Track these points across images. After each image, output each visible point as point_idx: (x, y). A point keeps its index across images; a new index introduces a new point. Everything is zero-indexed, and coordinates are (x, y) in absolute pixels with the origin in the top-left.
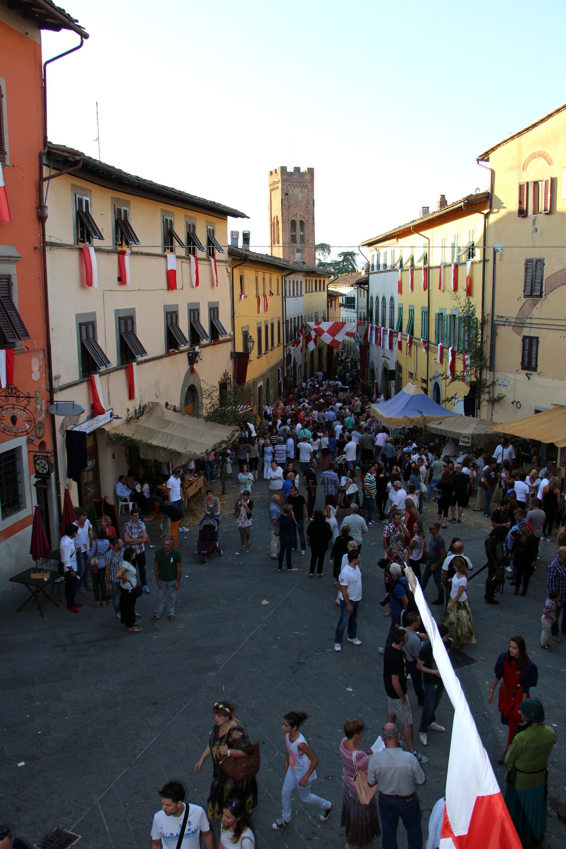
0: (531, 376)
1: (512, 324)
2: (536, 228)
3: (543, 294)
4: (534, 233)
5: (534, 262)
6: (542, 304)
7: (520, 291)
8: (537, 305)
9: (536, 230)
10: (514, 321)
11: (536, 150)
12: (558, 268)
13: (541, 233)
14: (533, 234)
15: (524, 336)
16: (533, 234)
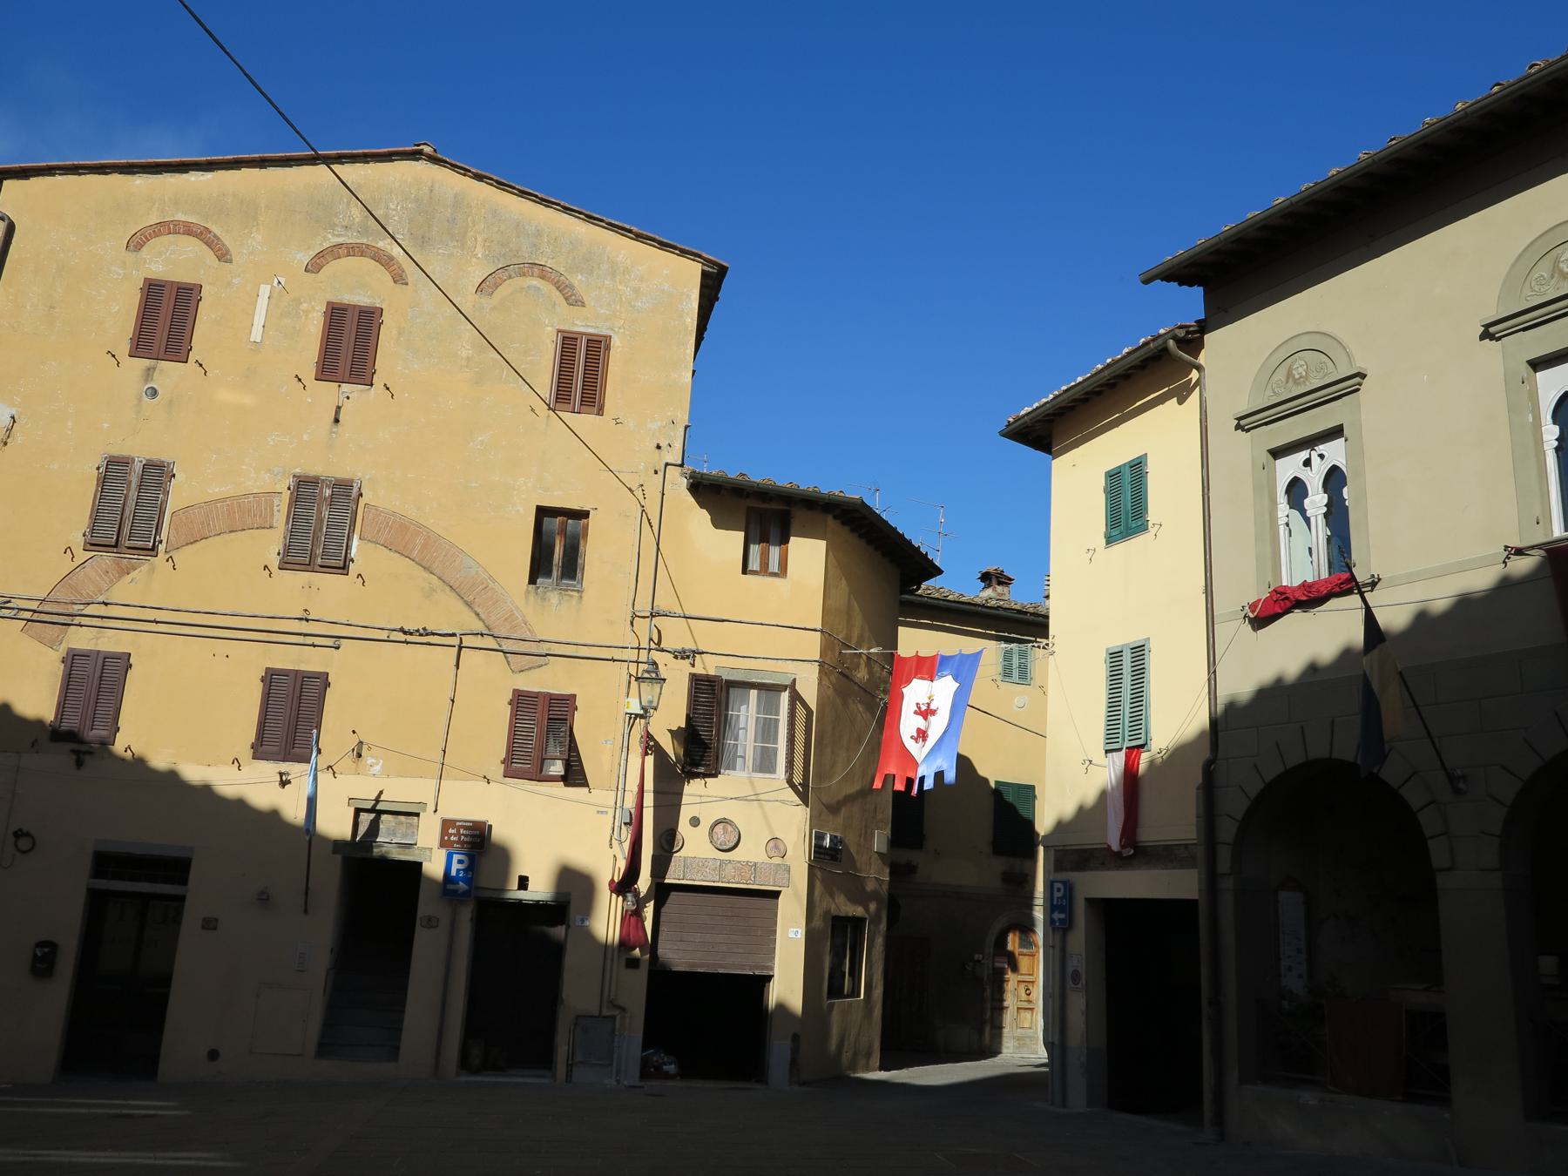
0: (87, 758)
1: (27, 615)
2: (153, 388)
3: (161, 548)
4: (145, 398)
5: (138, 467)
6: (152, 570)
7: (76, 530)
8: (133, 574)
9: (154, 393)
10: (34, 605)
11: (180, 217)
12: (216, 491)
13: (171, 401)
14: (140, 400)
15: (70, 650)
16: (140, 400)
